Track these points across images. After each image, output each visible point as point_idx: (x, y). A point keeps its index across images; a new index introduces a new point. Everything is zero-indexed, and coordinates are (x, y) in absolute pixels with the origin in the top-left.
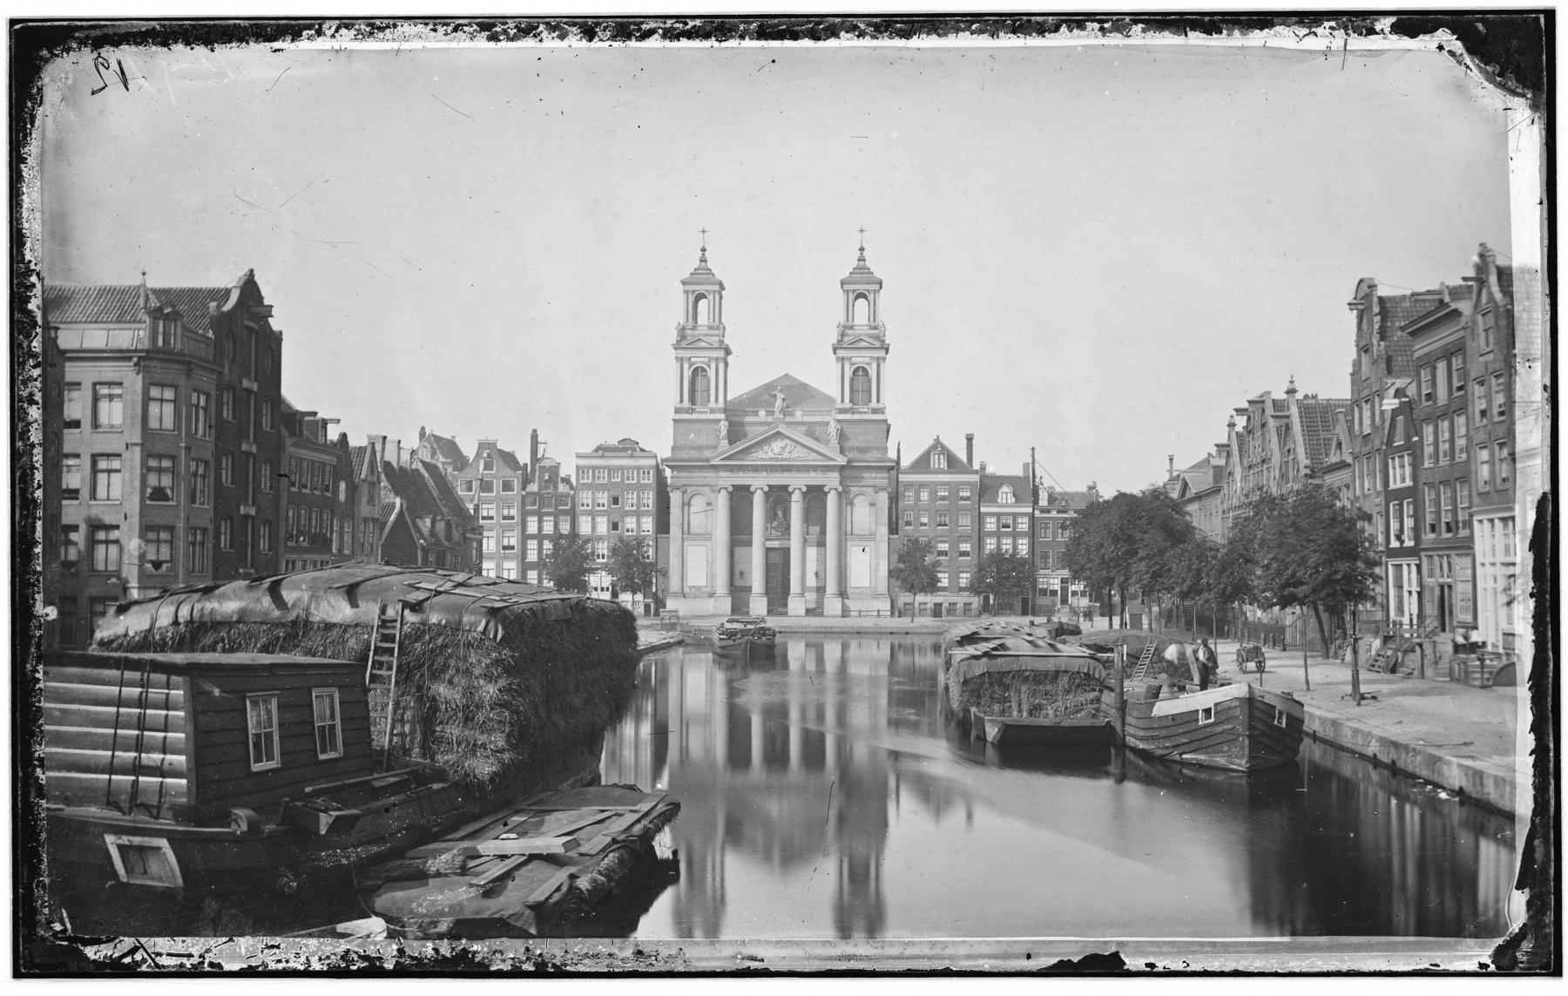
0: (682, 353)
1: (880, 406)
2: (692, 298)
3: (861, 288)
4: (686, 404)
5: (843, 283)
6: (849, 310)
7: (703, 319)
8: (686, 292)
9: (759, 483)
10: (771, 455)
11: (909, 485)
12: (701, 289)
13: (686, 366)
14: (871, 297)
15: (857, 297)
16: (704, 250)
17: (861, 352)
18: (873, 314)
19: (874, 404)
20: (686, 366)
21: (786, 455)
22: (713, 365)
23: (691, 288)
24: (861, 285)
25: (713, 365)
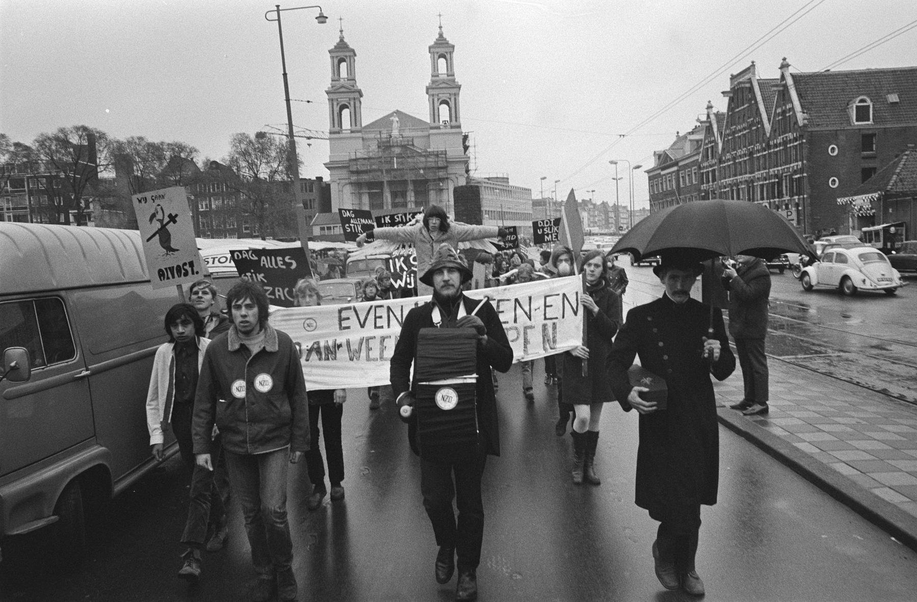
0: (334, 96)
1: (457, 124)
2: (336, 61)
3: (442, 50)
4: (337, 128)
5: (430, 48)
6: (435, 67)
7: (344, 73)
8: (332, 57)
12: (341, 55)
13: (335, 103)
14: (448, 56)
15: (439, 57)
17: (445, 91)
18: (450, 66)
19: (454, 123)
22: (352, 103)
23: (334, 55)
24: (442, 49)
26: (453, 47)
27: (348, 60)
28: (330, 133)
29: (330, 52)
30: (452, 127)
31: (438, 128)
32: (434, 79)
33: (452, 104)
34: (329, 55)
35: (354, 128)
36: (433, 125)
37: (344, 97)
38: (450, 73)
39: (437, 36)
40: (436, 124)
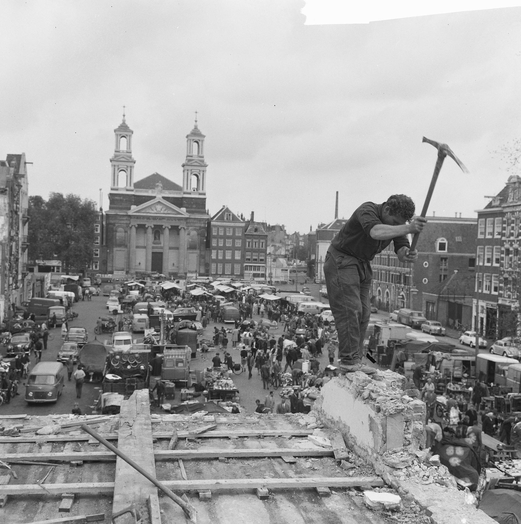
1: (203, 192)
3: (196, 138)
6: (190, 148)
7: (123, 147)
9: (150, 224)
10: (155, 211)
11: (215, 226)
13: (116, 169)
14: (200, 143)
16: (124, 116)
19: (201, 191)
20: (116, 169)
21: (162, 212)
22: (129, 169)
25: (129, 169)
26: (204, 136)
27: (128, 138)
28: (112, 189)
29: (115, 131)
30: (200, 194)
31: (190, 194)
32: (189, 158)
33: (201, 177)
34: (114, 134)
35: (128, 188)
36: (185, 190)
37: (122, 161)
38: (200, 155)
39: (193, 128)
40: (189, 191)
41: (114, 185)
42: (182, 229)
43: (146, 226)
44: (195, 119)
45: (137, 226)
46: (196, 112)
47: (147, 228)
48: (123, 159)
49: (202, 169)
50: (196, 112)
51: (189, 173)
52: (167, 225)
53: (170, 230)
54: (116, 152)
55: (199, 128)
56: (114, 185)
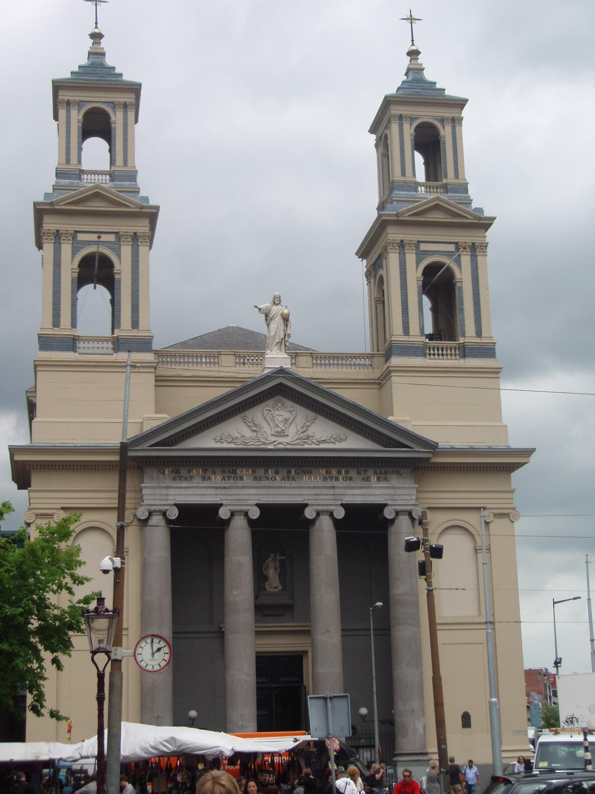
3: (427, 114)
9: (240, 499)
16: (96, 37)
41: (56, 323)
42: (404, 520)
43: (224, 513)
44: (408, 47)
45: (174, 514)
46: (411, 19)
47: (227, 523)
48: (97, 205)
49: (466, 237)
50: (411, 19)
51: (411, 258)
52: (324, 499)
53: (337, 523)
54: (59, 174)
55: (428, 76)
56: (56, 323)
